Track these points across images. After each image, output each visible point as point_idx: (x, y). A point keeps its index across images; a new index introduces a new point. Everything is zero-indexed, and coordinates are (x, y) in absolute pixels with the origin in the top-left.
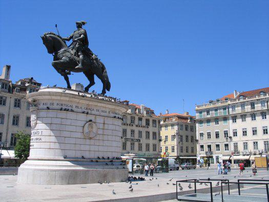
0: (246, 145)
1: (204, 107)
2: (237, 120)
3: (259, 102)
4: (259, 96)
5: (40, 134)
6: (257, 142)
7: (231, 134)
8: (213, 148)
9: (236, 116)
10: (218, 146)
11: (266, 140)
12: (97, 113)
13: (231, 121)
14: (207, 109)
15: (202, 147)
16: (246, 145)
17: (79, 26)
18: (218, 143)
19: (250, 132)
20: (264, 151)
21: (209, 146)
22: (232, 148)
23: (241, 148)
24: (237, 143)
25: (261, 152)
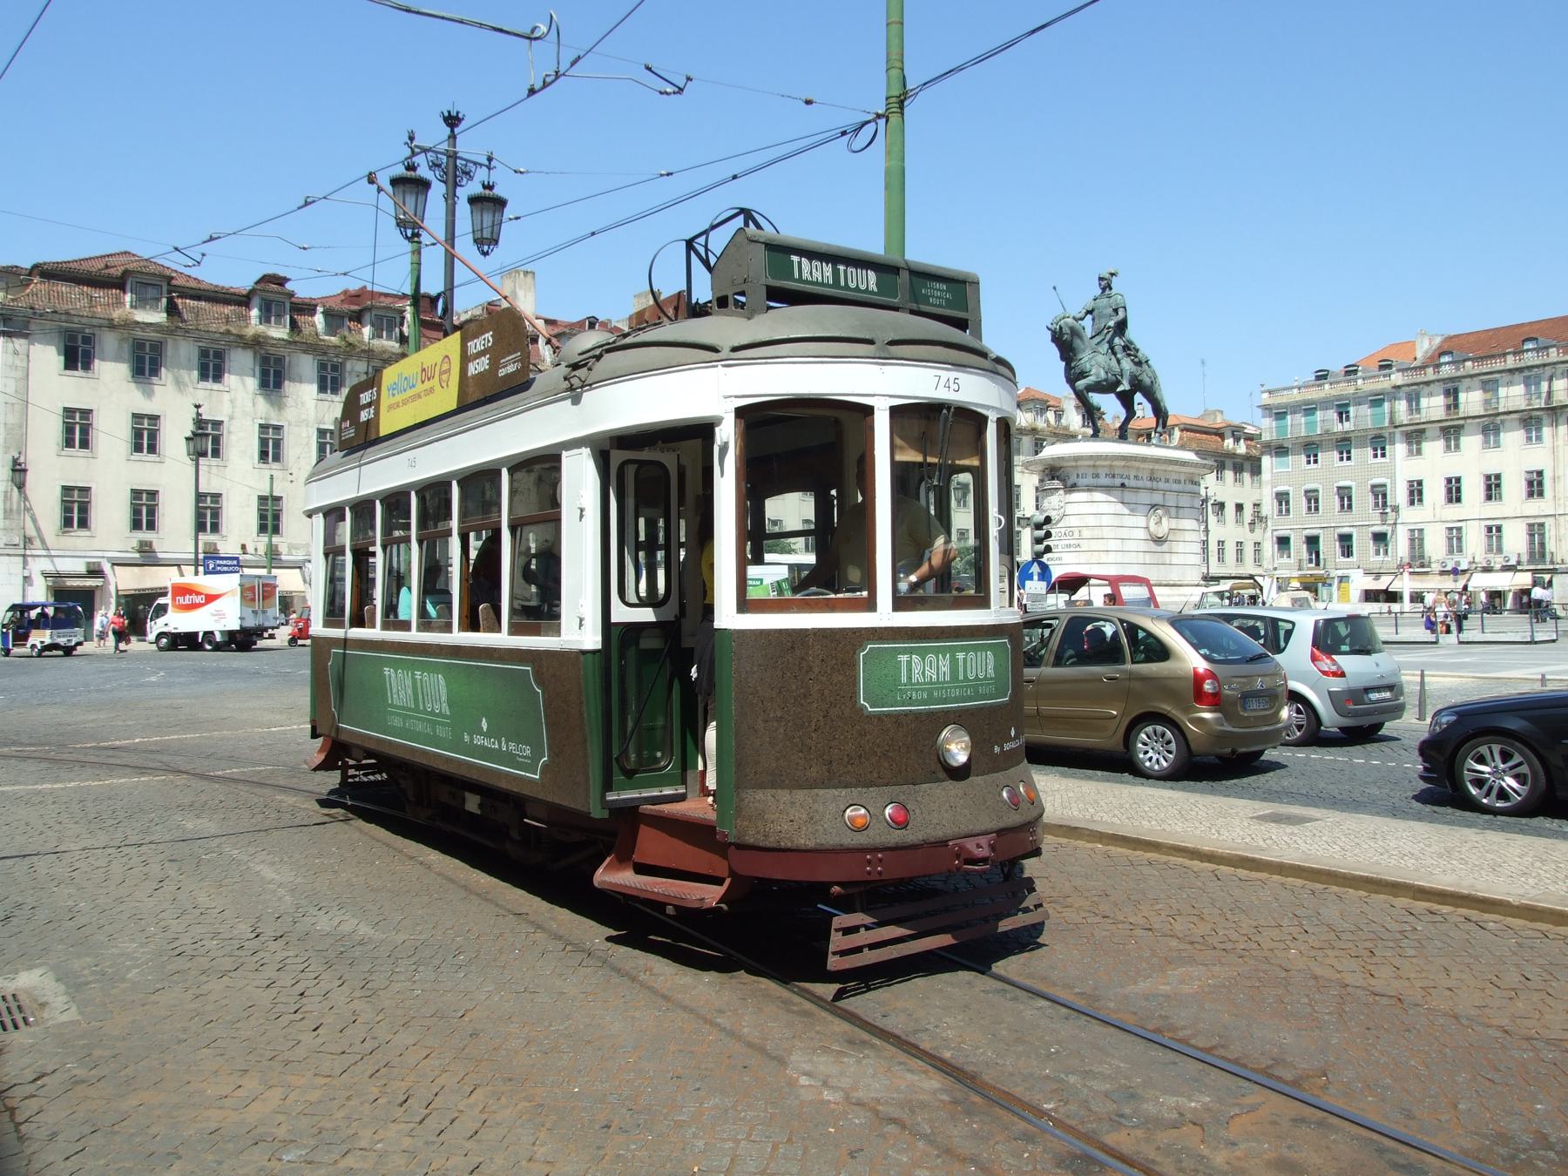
0: (1455, 538)
1: (1295, 396)
2: (1426, 446)
3: (1517, 377)
4: (1518, 352)
5: (1076, 535)
6: (1499, 529)
7: (1400, 495)
8: (1329, 547)
9: (1423, 431)
10: (1345, 540)
11: (1532, 521)
12: (1166, 486)
13: (1399, 449)
14: (1307, 403)
15: (1283, 542)
16: (1455, 538)
17: (1106, 285)
18: (1346, 530)
19: (1473, 489)
20: (1525, 558)
21: (1312, 541)
22: (1401, 546)
23: (1435, 546)
24: (1421, 530)
25: (1513, 562)
